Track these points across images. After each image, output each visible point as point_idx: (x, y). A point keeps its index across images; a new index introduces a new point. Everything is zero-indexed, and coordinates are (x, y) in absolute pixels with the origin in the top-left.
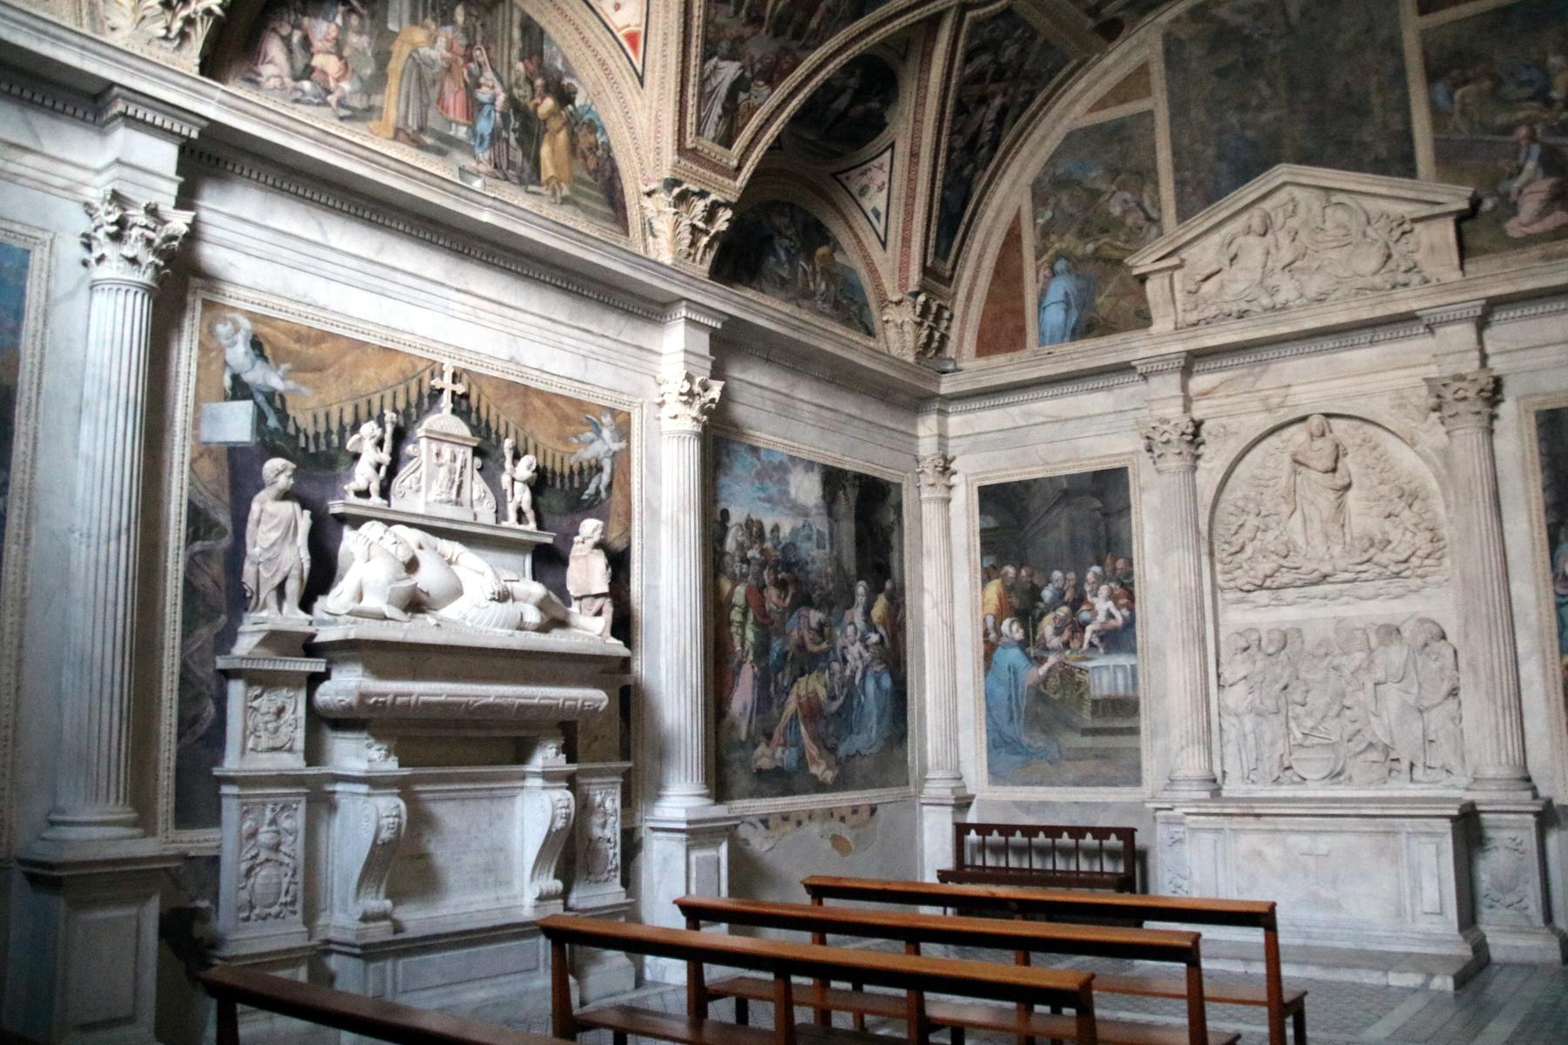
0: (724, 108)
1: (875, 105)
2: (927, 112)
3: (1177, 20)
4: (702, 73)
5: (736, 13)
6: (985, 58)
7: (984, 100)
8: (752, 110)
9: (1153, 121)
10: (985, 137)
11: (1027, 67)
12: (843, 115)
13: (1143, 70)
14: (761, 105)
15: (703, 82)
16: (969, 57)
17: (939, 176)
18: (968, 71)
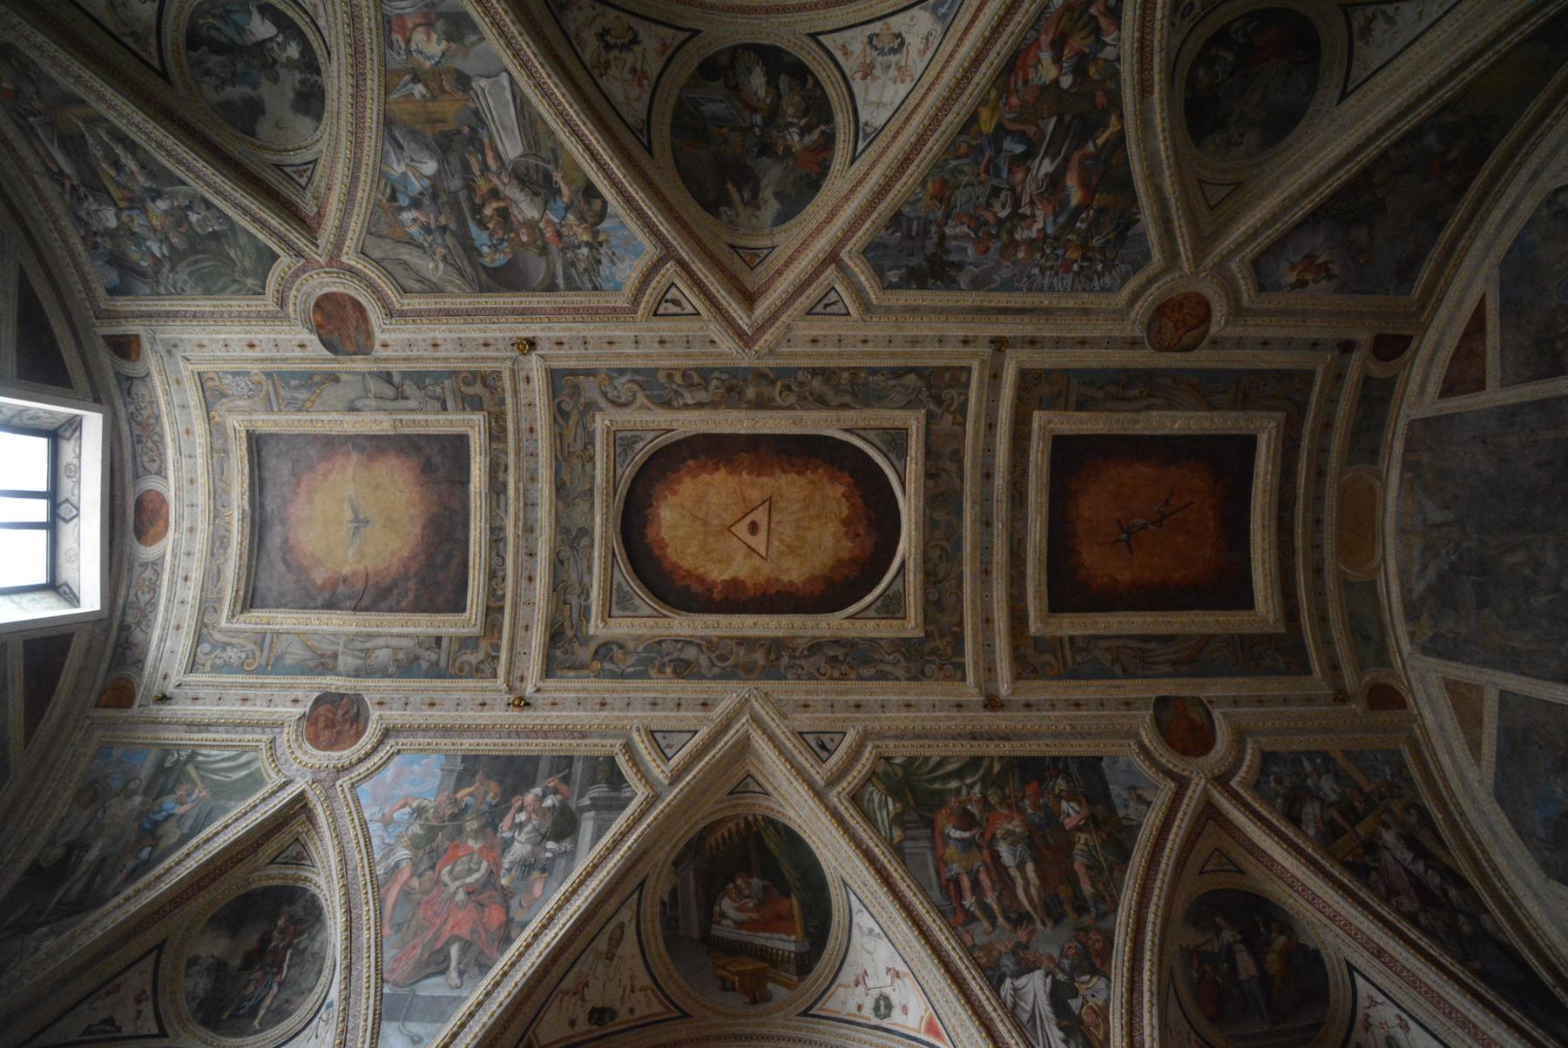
0: (1061, 1028)
1: (1280, 941)
2: (1326, 898)
3: (1412, 634)
4: (1003, 1004)
5: (994, 924)
6: (1311, 810)
7: (1372, 846)
8: (1102, 1013)
10: (1434, 880)
11: (1367, 788)
13: (1452, 687)
14: (1107, 1001)
15: (1012, 1013)
16: (1295, 821)
17: (1434, 951)
18: (1311, 832)
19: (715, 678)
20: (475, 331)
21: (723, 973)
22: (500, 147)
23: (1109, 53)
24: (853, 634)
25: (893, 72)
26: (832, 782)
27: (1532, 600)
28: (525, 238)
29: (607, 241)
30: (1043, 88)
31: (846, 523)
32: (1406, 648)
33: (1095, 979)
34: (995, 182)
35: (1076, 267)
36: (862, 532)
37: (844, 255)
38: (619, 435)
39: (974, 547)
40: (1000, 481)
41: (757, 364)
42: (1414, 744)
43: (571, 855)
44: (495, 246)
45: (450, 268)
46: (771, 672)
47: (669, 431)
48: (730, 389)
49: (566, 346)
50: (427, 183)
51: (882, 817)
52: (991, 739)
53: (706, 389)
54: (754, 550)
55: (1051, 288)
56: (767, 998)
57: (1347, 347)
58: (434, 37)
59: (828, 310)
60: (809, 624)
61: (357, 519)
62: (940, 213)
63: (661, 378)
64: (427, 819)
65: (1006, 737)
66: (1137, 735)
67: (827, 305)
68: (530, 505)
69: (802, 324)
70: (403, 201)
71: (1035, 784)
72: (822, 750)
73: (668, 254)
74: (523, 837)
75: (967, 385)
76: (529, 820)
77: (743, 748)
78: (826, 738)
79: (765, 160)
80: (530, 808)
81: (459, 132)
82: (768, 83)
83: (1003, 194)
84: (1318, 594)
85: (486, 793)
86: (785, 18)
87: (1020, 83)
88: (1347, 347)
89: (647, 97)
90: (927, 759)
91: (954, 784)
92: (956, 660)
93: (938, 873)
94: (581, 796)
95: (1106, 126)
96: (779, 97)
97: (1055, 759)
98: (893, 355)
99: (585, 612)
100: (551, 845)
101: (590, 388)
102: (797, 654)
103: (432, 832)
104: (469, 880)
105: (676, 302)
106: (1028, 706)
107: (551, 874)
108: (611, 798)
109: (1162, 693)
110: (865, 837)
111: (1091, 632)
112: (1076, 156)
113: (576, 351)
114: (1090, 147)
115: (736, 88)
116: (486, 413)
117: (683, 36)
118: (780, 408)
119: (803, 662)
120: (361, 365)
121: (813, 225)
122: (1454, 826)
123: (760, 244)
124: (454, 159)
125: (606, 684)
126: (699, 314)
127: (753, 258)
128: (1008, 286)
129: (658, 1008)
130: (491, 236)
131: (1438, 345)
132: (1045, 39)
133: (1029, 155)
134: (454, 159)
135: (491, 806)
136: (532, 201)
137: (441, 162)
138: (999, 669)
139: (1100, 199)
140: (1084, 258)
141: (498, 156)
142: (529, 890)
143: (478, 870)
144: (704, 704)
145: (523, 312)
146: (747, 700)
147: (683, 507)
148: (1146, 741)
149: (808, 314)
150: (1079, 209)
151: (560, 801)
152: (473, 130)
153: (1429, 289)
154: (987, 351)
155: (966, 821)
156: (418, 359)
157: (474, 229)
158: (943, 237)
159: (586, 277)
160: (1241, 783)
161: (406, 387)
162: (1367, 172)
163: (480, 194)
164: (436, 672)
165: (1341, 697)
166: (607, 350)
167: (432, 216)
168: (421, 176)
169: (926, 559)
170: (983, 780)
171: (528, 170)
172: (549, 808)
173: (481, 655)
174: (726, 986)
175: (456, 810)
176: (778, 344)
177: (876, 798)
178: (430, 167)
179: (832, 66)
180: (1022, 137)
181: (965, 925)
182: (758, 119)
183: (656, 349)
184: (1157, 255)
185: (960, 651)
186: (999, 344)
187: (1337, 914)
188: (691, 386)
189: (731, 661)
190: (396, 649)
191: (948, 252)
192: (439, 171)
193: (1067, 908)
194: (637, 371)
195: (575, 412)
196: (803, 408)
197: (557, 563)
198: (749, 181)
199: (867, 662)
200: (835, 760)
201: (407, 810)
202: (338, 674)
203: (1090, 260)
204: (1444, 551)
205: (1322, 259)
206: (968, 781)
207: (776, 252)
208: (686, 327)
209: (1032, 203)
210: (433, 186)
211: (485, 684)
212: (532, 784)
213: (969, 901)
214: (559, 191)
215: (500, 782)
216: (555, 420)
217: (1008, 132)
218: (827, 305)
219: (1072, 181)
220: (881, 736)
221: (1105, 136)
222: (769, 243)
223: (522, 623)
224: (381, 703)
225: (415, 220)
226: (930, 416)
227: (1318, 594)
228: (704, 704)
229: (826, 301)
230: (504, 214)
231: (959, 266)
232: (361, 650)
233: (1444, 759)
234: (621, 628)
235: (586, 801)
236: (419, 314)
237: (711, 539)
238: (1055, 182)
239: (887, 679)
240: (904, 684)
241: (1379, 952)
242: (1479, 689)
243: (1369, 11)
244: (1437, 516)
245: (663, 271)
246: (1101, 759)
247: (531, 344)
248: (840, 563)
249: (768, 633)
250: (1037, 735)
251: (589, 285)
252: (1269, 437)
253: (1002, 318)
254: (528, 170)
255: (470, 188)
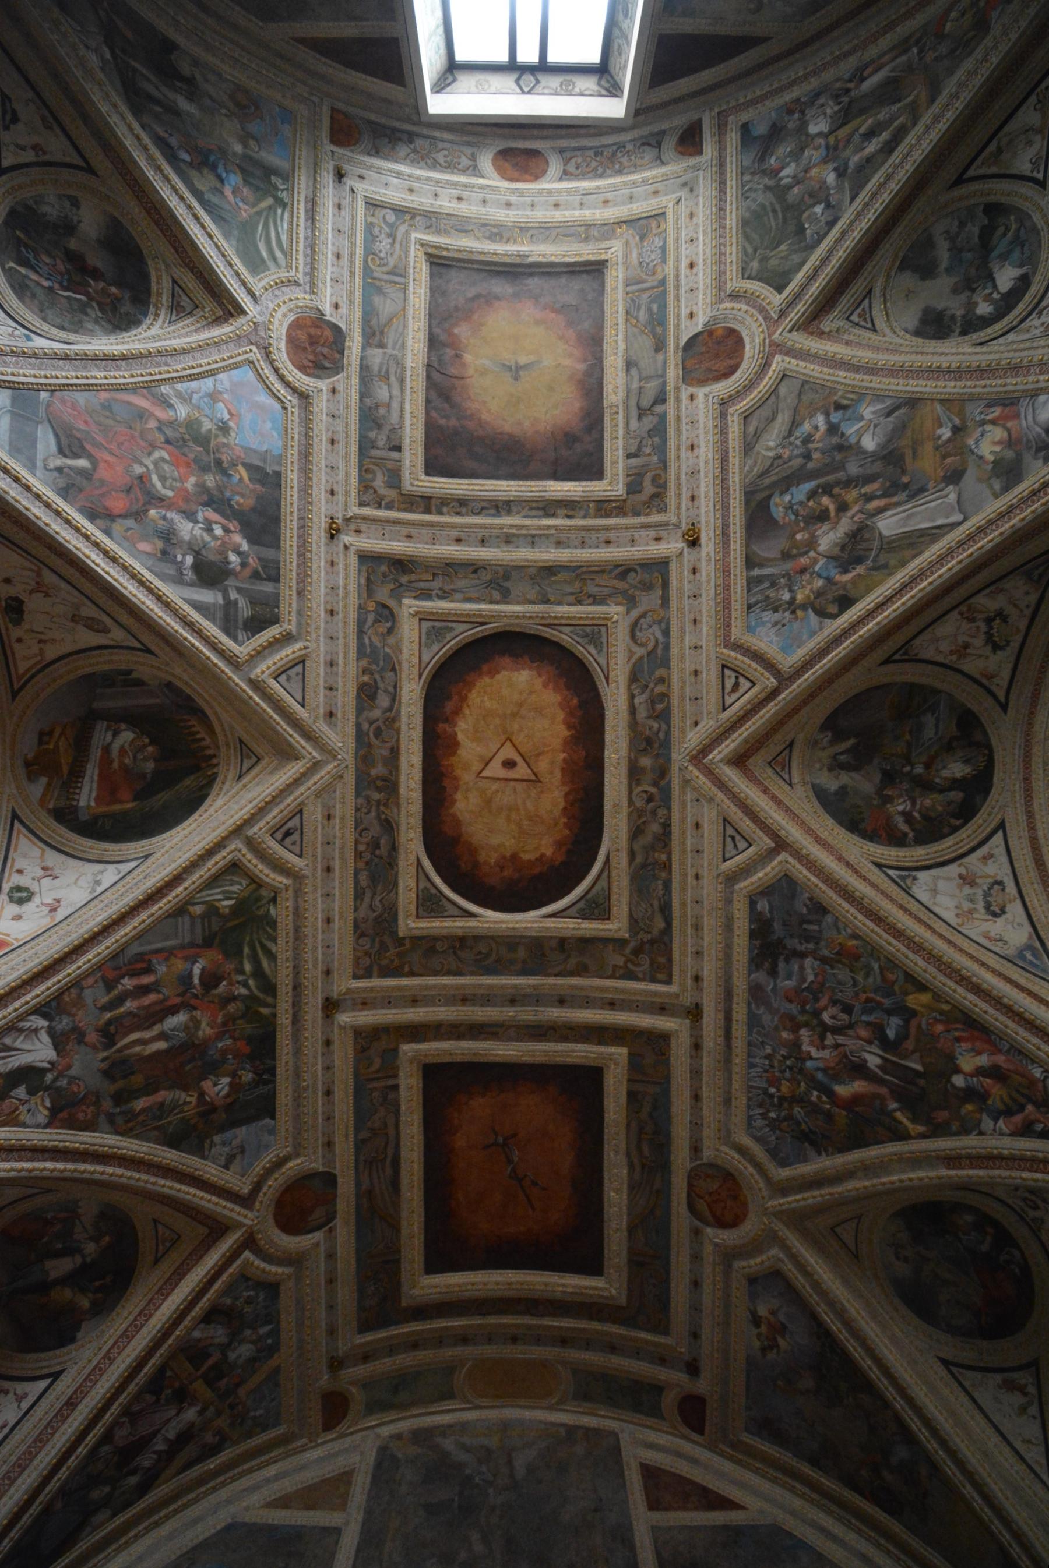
1: (85, 1304)
2: (127, 1350)
3: (399, 1437)
4: (22, 1018)
5: (104, 1008)
6: (219, 1333)
7: (182, 1397)
9: (337, 1543)
10: (146, 1461)
11: (242, 1392)
12: (45, 1287)
13: (345, 1478)
14: (24, 1125)
16: (208, 1318)
17: (72, 1462)
18: (197, 1334)
19: (358, 725)
20: (706, 487)
21: (57, 734)
22: (889, 513)
23: (987, 1124)
24: (402, 864)
25: (966, 905)
26: (251, 844)
27: (434, 1560)
28: (799, 537)
29: (796, 618)
30: (951, 1058)
31: (514, 857)
32: (386, 1431)
33: (46, 1112)
34: (857, 1008)
35: (772, 1090)
36: (506, 873)
37: (784, 856)
38: (603, 629)
39: (491, 987)
40: (556, 1014)
41: (675, 768)
42: (285, 1440)
43: (179, 580)
44: (791, 507)
45: (769, 463)
46: (364, 782)
47: (607, 679)
48: (649, 741)
49: (692, 576)
50: (853, 440)
51: (215, 895)
52: (294, 1005)
53: (649, 717)
54: (487, 764)
55: (751, 1066)
56: (31, 777)
57: (693, 1368)
58: (998, 449)
59: (729, 840)
60: (412, 821)
61: (519, 368)
62: (825, 952)
63: (660, 672)
64: (216, 436)
65: (296, 1020)
66: (297, 1155)
67: (733, 838)
68: (533, 540)
69: (714, 813)
70: (835, 417)
71: (247, 1050)
72: (284, 833)
73: (784, 679)
74: (197, 532)
75: (653, 980)
76: (215, 538)
77: (287, 753)
78: (296, 836)
79: (877, 778)
80: (227, 539)
81: (904, 472)
82: (955, 780)
83: (845, 1017)
84: (440, 1340)
85: (243, 495)
86: (1019, 797)
87: (956, 1034)
88: (693, 1368)
89: (940, 659)
90: (274, 940)
91: (248, 967)
92: (375, 969)
93: (157, 951)
94: (239, 590)
95: (914, 1120)
96: (941, 791)
97: (272, 1071)
98: (683, 904)
99: (425, 595)
100: (189, 560)
101: (649, 601)
102: (382, 808)
103: (203, 441)
104: (155, 478)
105: (736, 686)
106: (328, 1043)
107: (160, 560)
108: (236, 621)
109: (340, 1180)
110: (195, 877)
111: (403, 1108)
112: (884, 1091)
113: (686, 586)
114: (894, 1105)
115: (949, 748)
116: (625, 497)
117: (1001, 696)
118: (630, 792)
119: (373, 814)
120: (673, 374)
121: (813, 825)
122: (201, 1481)
123: (795, 773)
124: (877, 467)
125: (352, 615)
126: (724, 709)
127: (781, 764)
128: (753, 1021)
129: (23, 666)
130: (801, 503)
131: (694, 1461)
132: (1000, 1059)
133: (886, 1044)
134: (877, 467)
135: (229, 500)
136: (836, 545)
137: (873, 454)
138: (365, 1013)
139: (841, 1116)
140: (782, 1099)
141: (881, 511)
142: (145, 538)
143: (164, 487)
144: (331, 714)
145: (725, 534)
146: (335, 757)
147: (531, 693)
148: (290, 1164)
149: (725, 820)
150: (831, 1094)
151: (234, 569)
152: (906, 486)
153: (750, 1452)
154: (687, 1000)
155: (211, 980)
156: (678, 430)
157: (808, 486)
158: (802, 955)
159: (759, 597)
160: (247, 1263)
161: (650, 417)
162: (869, 1387)
163: (843, 492)
164: (365, 446)
165: (336, 1364)
166: (688, 618)
167: (820, 445)
168: (860, 434)
169: (477, 938)
170: (252, 997)
171: (868, 540)
172: (226, 558)
173: (382, 491)
174: (43, 736)
175: (225, 465)
176: (694, 789)
177: (235, 888)
178: (869, 443)
179: (975, 843)
180: (903, 1036)
181: (104, 979)
182: (919, 770)
183: (689, 667)
184: (785, 1173)
185: (385, 973)
186: (695, 1013)
187: (112, 1361)
188: (652, 702)
189: (373, 740)
190: (388, 406)
191: (787, 961)
192: (865, 452)
193: (120, 1084)
194: (667, 647)
195: (626, 586)
196: (630, 814)
197: (475, 568)
198: (857, 760)
199: (373, 879)
200: (274, 846)
201: (226, 416)
202: (364, 348)
203: (780, 1105)
204: (484, 1469)
205: (781, 1342)
206: (251, 982)
207: (786, 787)
208: (711, 698)
209: (837, 1046)
210: (850, 447)
211: (353, 494)
212: (251, 541)
213: (127, 983)
214: (846, 571)
215: (254, 509)
216: (617, 566)
217: (907, 1022)
218: (733, 838)
219: (858, 1086)
220: (298, 892)
221: (904, 1120)
222: (795, 780)
223: (414, 532)
224: (334, 391)
225: (816, 428)
226: (621, 943)
227: (440, 1340)
228: (331, 714)
229: (738, 838)
230: (823, 516)
231: (773, 973)
232: (387, 372)
233: (272, 1471)
234: (409, 631)
235: (233, 595)
236: (723, 432)
237: (497, 721)
238: (859, 1070)
239: (356, 899)
240: (351, 917)
241: (72, 1404)
242: (343, 1506)
243: (1032, 1390)
244: (520, 1462)
245: (767, 674)
246: (273, 1117)
247: (694, 543)
248: (473, 851)
249: (403, 778)
250: (297, 1052)
251: (753, 600)
252: (601, 1289)
253: (721, 1016)
254: (868, 540)
255: (849, 483)
